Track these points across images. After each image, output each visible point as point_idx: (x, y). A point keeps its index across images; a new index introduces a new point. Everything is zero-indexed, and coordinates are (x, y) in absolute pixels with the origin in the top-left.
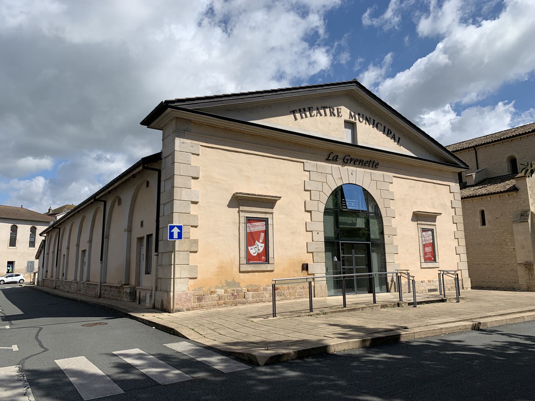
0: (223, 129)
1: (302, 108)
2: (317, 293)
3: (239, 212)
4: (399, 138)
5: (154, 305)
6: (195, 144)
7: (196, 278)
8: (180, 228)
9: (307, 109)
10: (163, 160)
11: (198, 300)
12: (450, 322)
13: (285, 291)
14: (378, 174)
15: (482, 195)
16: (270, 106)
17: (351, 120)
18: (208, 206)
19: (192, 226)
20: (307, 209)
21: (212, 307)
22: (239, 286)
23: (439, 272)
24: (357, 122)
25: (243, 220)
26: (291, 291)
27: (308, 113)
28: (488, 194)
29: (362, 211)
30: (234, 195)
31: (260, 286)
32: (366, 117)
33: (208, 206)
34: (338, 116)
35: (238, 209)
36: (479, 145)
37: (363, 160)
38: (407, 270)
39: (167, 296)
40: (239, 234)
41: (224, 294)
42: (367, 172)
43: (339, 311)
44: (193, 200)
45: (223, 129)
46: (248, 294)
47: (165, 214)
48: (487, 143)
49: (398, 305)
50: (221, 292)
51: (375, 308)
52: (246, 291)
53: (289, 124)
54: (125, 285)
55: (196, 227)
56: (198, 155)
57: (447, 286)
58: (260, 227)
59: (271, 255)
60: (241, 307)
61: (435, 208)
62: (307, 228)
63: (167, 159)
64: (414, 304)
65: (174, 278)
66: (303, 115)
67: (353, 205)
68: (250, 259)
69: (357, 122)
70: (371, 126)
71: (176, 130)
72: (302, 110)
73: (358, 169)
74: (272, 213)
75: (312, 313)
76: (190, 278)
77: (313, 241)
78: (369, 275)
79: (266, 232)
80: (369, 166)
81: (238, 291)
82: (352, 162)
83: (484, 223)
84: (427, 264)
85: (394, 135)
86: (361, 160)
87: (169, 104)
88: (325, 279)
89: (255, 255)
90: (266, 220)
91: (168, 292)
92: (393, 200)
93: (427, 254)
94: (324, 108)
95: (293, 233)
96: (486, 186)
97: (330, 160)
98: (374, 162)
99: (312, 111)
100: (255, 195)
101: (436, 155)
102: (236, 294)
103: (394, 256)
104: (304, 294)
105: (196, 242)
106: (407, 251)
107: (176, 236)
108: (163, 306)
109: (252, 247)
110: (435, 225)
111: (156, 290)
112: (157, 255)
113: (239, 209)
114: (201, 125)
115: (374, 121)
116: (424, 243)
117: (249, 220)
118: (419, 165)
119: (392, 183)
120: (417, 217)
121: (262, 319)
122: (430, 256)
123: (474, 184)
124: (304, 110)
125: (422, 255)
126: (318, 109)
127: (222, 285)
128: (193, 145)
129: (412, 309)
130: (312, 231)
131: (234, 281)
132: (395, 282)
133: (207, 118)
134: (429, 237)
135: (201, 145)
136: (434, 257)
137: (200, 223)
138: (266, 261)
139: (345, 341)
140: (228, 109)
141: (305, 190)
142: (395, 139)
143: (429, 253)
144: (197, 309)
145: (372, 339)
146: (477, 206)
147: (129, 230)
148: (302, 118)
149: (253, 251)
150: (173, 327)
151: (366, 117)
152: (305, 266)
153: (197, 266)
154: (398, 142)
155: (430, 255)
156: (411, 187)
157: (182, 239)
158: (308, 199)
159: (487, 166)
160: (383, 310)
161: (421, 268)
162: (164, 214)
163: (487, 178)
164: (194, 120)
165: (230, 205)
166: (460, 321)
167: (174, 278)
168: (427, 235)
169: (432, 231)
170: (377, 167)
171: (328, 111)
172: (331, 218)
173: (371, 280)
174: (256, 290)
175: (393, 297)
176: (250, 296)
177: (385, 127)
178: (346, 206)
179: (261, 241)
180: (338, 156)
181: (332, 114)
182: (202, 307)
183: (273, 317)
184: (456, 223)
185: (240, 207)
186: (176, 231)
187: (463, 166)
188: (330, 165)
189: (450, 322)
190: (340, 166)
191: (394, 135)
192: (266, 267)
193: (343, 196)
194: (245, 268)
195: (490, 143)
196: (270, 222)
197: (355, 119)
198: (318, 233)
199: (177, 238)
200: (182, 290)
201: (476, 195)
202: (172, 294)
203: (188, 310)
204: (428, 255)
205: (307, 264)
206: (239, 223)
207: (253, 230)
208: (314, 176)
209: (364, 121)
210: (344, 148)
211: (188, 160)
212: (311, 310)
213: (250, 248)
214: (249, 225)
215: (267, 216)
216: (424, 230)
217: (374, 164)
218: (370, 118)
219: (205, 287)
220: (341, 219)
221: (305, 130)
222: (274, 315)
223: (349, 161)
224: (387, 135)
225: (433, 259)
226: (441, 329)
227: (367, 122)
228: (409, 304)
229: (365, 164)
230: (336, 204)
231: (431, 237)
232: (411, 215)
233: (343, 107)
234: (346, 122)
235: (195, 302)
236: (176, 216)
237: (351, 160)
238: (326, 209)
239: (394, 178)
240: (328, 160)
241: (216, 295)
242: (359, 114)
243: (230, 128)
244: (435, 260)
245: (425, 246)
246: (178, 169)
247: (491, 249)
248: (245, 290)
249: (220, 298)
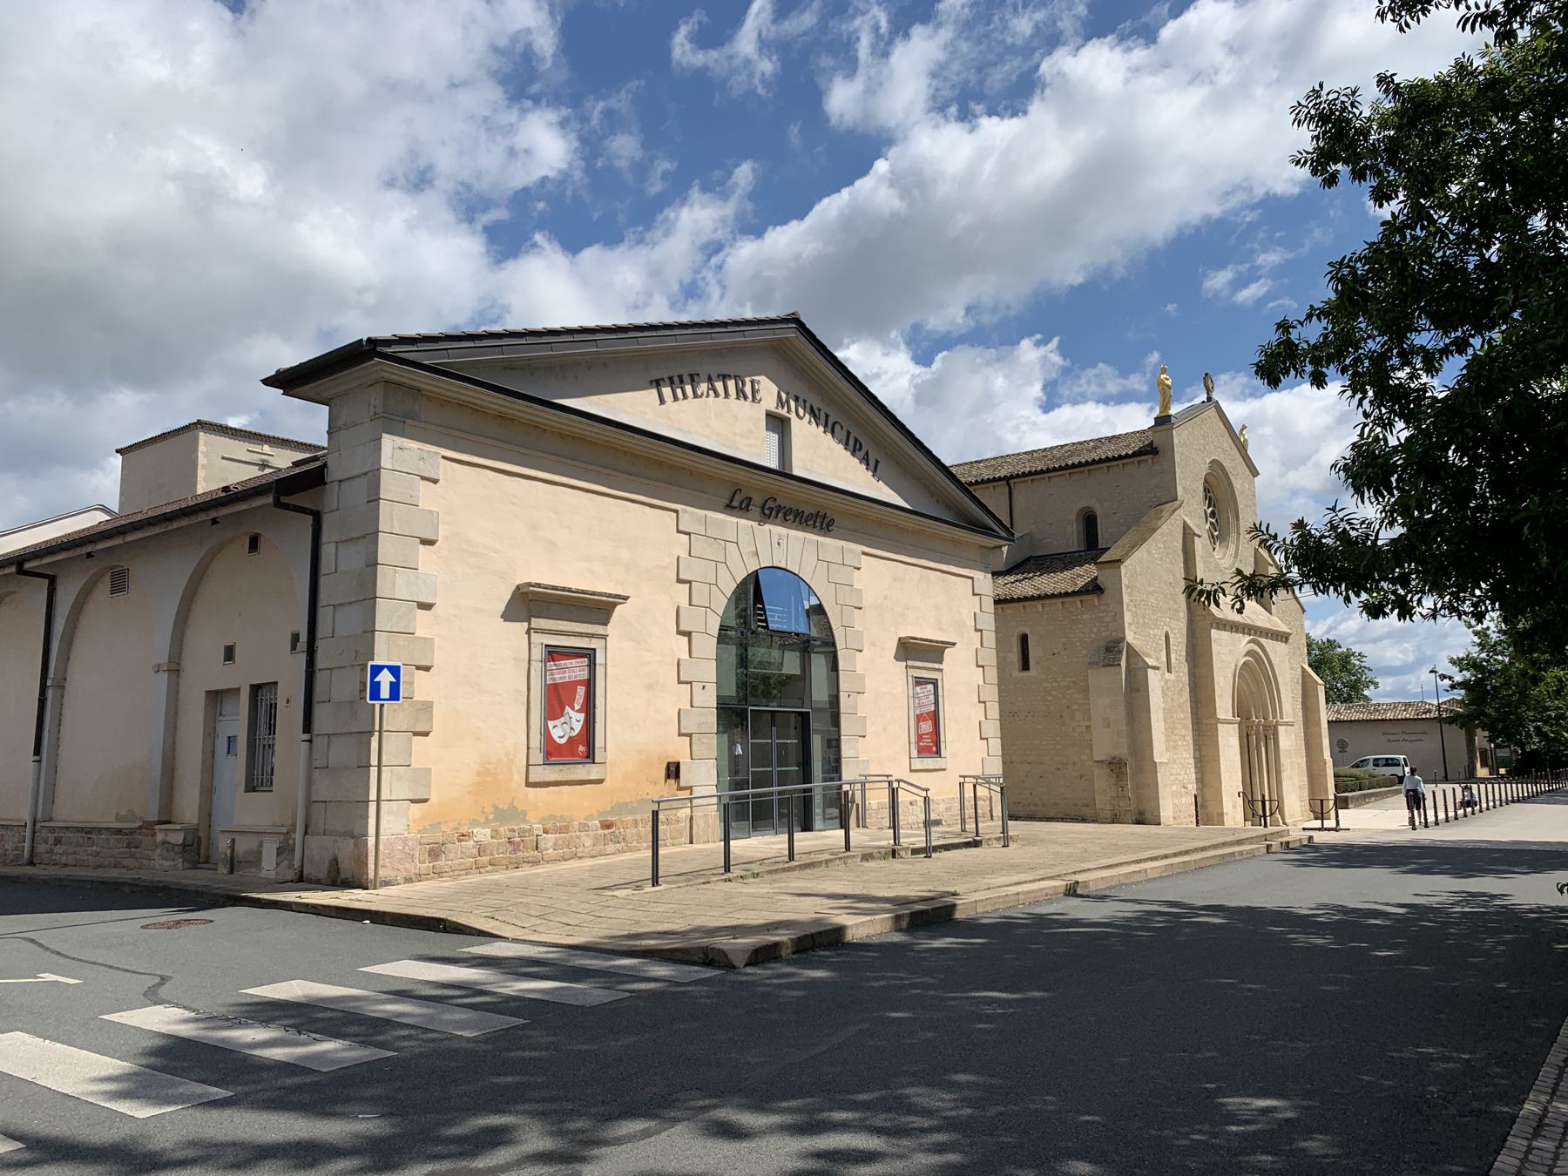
0: (495, 417)
1: (675, 373)
2: (698, 833)
3: (528, 633)
4: (877, 462)
5: (302, 872)
6: (428, 451)
7: (425, 801)
8: (395, 671)
9: (686, 378)
10: (332, 490)
11: (429, 855)
12: (1026, 882)
13: (628, 831)
14: (830, 543)
15: (1026, 599)
16: (605, 365)
17: (780, 411)
18: (455, 616)
19: (418, 668)
20: (682, 628)
21: (464, 872)
22: (525, 821)
23: (962, 780)
24: (793, 416)
25: (538, 653)
26: (641, 829)
27: (688, 388)
28: (1040, 597)
29: (797, 634)
30: (518, 588)
31: (572, 820)
32: (811, 406)
33: (455, 616)
34: (753, 401)
35: (526, 624)
36: (1018, 476)
38: (888, 776)
39: (356, 845)
40: (529, 689)
41: (491, 840)
42: (810, 541)
43: (784, 870)
45: (495, 417)
46: (545, 839)
47: (338, 633)
48: (1036, 473)
49: (894, 853)
50: (483, 834)
51: (850, 861)
52: (541, 833)
53: (646, 414)
54: (160, 823)
55: (427, 669)
56: (435, 481)
58: (575, 670)
59: (599, 743)
60: (526, 871)
61: (941, 629)
62: (681, 674)
63: (344, 485)
64: (927, 851)
65: (378, 801)
66: (679, 391)
67: (776, 618)
68: (553, 752)
69: (793, 416)
70: (821, 429)
71: (385, 415)
72: (676, 380)
73: (793, 533)
74: (604, 637)
75: (729, 875)
76: (413, 801)
77: (692, 706)
78: (805, 791)
79: (590, 684)
80: (815, 527)
81: (522, 833)
82: (780, 515)
83: (1025, 666)
85: (867, 453)
87: (379, 349)
88: (715, 800)
89: (563, 741)
90: (590, 654)
91: (359, 837)
92: (860, 608)
94: (724, 378)
95: (650, 687)
96: (1031, 575)
97: (734, 508)
98: (825, 516)
99: (699, 383)
100: (570, 590)
101: (950, 505)
102: (518, 839)
103: (857, 741)
104: (668, 835)
105: (427, 707)
106: (885, 729)
107: (385, 692)
108: (339, 873)
109: (557, 722)
110: (941, 670)
111: (306, 833)
112: (310, 741)
113: (529, 624)
114: (444, 402)
115: (827, 416)
116: (918, 713)
117: (553, 653)
119: (859, 569)
120: (910, 650)
121: (630, 891)
123: (1004, 569)
125: (913, 740)
126: (710, 379)
127: (487, 818)
128: (425, 455)
129: (921, 863)
130: (691, 683)
131: (513, 808)
132: (858, 805)
133: (460, 387)
135: (444, 457)
136: (937, 747)
137: (439, 659)
138: (588, 757)
139: (868, 918)
140: (509, 367)
141: (679, 581)
142: (868, 464)
144: (428, 879)
145: (911, 913)
146: (1014, 623)
147: (174, 668)
148: (676, 398)
149: (559, 733)
150: (442, 917)
151: (811, 406)
152: (673, 769)
153: (430, 769)
154: (875, 471)
156: (895, 579)
157: (398, 700)
158: (684, 603)
159: (1034, 526)
160: (866, 864)
161: (911, 771)
162: (333, 631)
163: (1031, 557)
164: (427, 390)
165: (508, 615)
166: (1042, 879)
167: (378, 801)
169: (935, 683)
170: (830, 528)
171: (731, 384)
172: (732, 650)
173: (807, 803)
174: (561, 830)
175: (867, 838)
176: (550, 844)
177: (849, 433)
178: (765, 621)
179: (577, 707)
180: (751, 498)
181: (741, 393)
182: (439, 874)
183: (653, 886)
184: (983, 667)
185: (533, 619)
186: (385, 678)
187: (1003, 534)
188: (735, 520)
189: (1026, 882)
190: (755, 524)
191: (867, 453)
192: (589, 773)
193: (758, 597)
194: (538, 774)
195: (1042, 472)
196: (599, 659)
198: (704, 687)
199: (388, 697)
200: (394, 832)
201: (1013, 598)
202: (371, 841)
203: (408, 880)
205: (679, 763)
206: (530, 660)
207: (560, 678)
208: (700, 545)
209: (807, 416)
211: (411, 493)
212: (727, 868)
213: (551, 724)
214: (551, 666)
215: (593, 644)
216: (919, 682)
217: (827, 520)
218: (819, 410)
219: (446, 822)
220: (758, 653)
221: (681, 430)
222: (655, 881)
223: (774, 513)
224: (853, 454)
225: (934, 748)
226: (1018, 894)
227: (813, 420)
228: (915, 852)
229: (806, 521)
230: (742, 615)
231: (932, 697)
232: (892, 646)
233: (764, 377)
234: (769, 415)
235: (424, 862)
236: (380, 640)
237: (779, 509)
238: (723, 628)
239: (863, 557)
240: (729, 508)
241: (472, 843)
242: (797, 399)
243: (513, 415)
244: (938, 753)
245: (919, 718)
246: (389, 517)
247: (1039, 727)
248: (539, 829)
249: (481, 849)
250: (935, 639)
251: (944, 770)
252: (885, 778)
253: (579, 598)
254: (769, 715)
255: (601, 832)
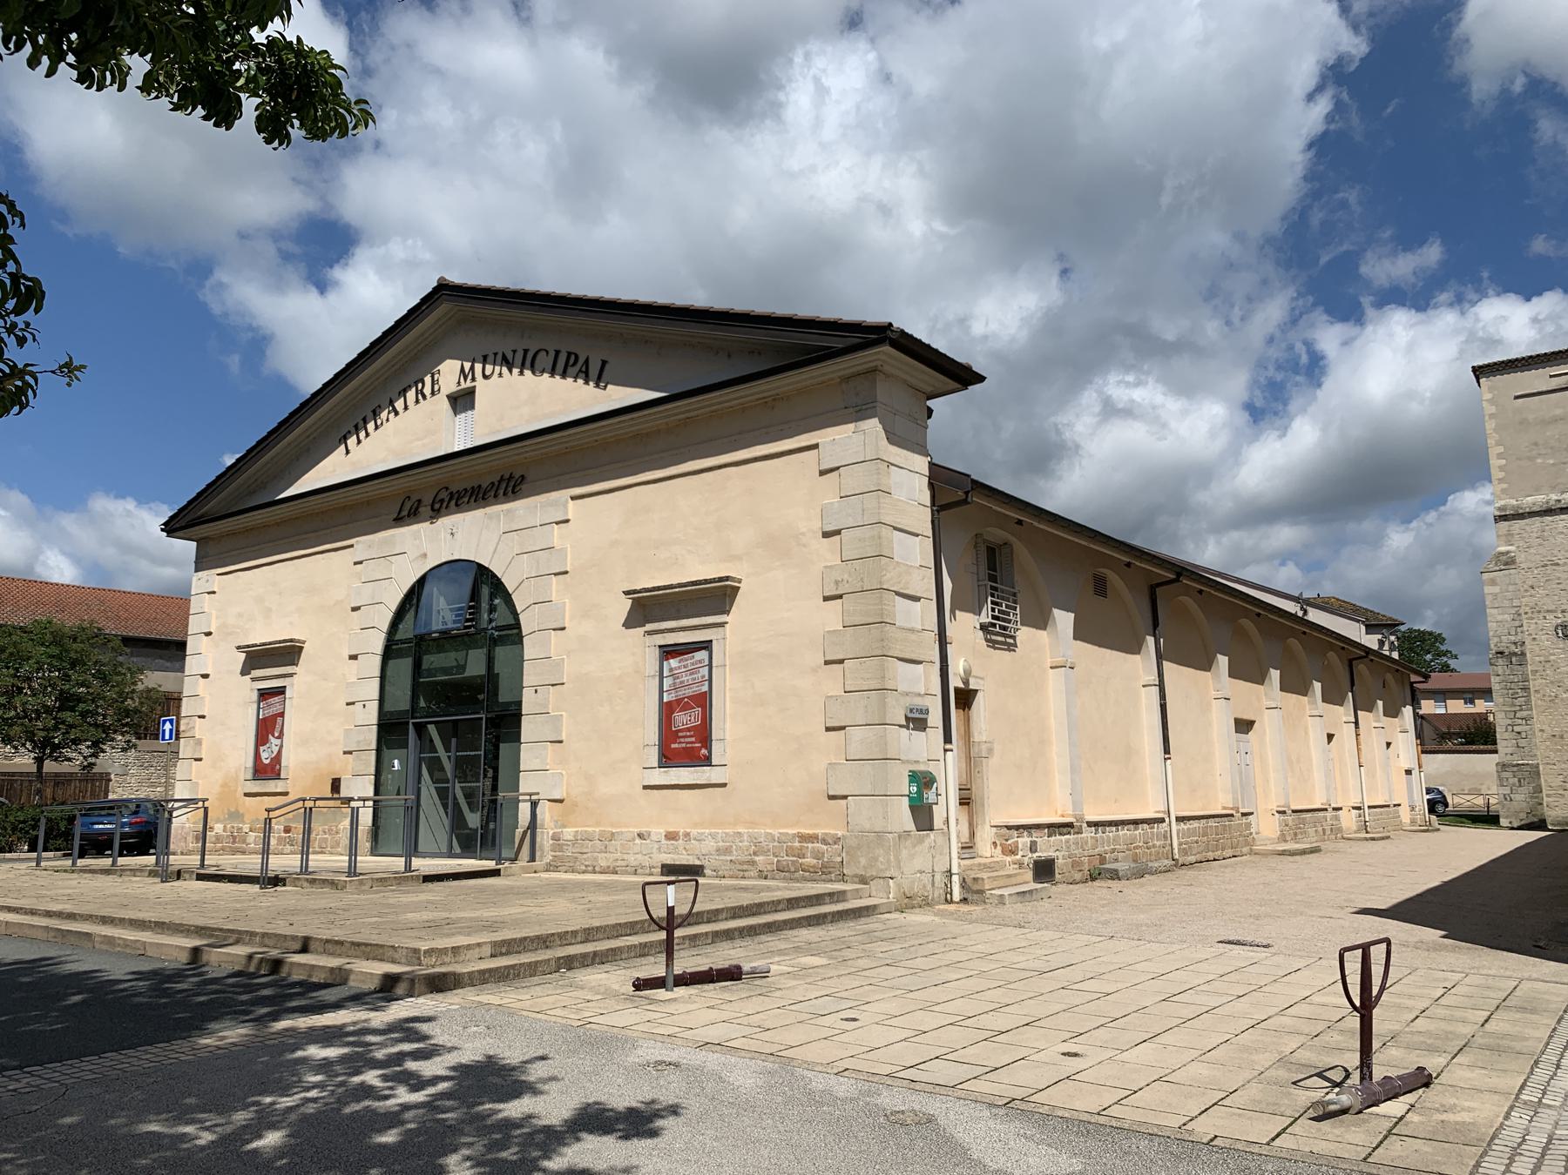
25: (255, 696)
37: (480, 486)
44: (202, 673)
57: (757, 858)
84: (665, 772)
86: (473, 488)
93: (680, 734)
94: (403, 392)
100: (256, 645)
118: (667, 424)
122: (692, 743)
124: (365, 422)
134: (692, 672)
135: (218, 575)
143: (688, 734)
155: (693, 739)
168: (685, 667)
180: (419, 501)
190: (426, 525)
192: (276, 787)
197: (473, 379)
198: (364, 706)
204: (682, 740)
210: (428, 475)
240: (399, 521)
242: (485, 360)
244: (707, 761)
250: (675, 582)
251: (645, 787)
252: (528, 797)
253: (254, 651)
254: (451, 724)
255: (283, 834)
